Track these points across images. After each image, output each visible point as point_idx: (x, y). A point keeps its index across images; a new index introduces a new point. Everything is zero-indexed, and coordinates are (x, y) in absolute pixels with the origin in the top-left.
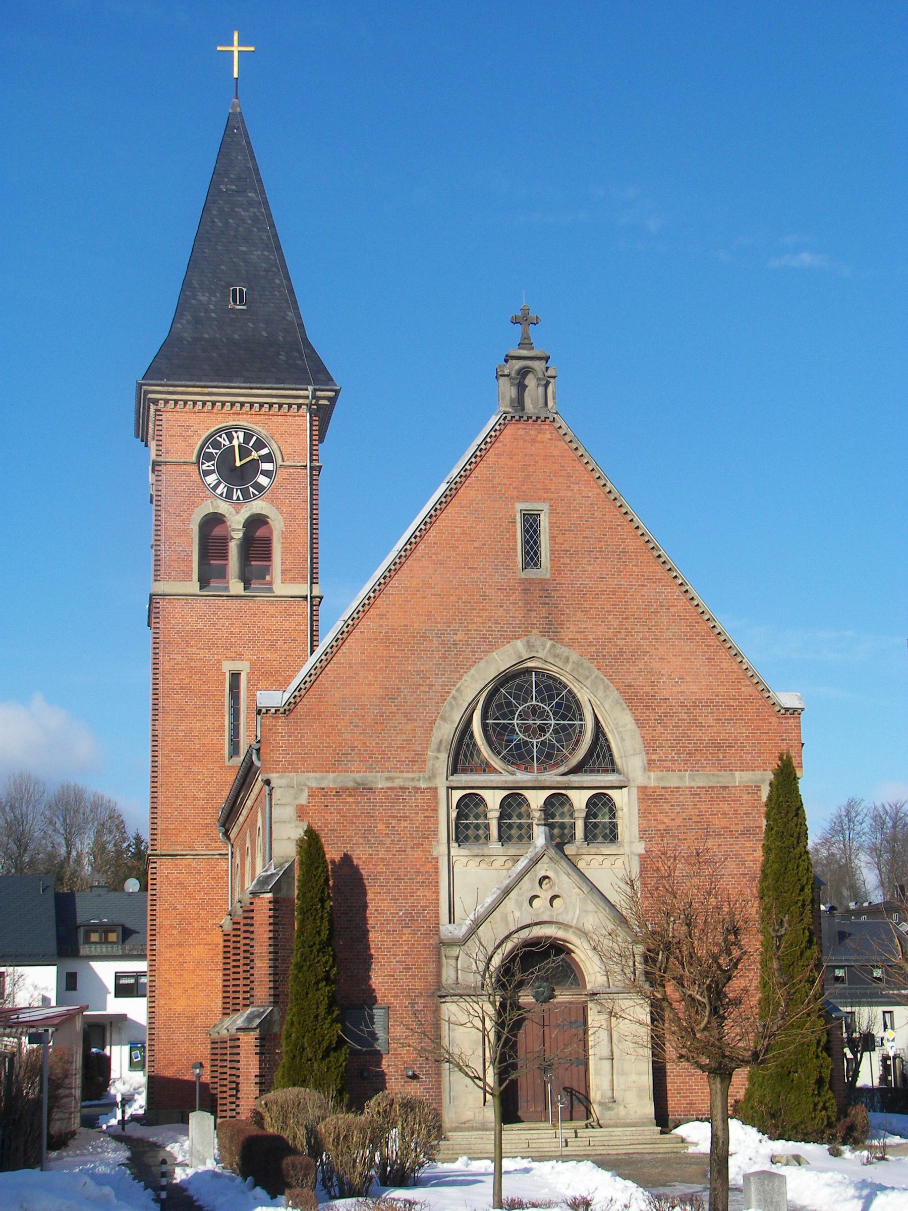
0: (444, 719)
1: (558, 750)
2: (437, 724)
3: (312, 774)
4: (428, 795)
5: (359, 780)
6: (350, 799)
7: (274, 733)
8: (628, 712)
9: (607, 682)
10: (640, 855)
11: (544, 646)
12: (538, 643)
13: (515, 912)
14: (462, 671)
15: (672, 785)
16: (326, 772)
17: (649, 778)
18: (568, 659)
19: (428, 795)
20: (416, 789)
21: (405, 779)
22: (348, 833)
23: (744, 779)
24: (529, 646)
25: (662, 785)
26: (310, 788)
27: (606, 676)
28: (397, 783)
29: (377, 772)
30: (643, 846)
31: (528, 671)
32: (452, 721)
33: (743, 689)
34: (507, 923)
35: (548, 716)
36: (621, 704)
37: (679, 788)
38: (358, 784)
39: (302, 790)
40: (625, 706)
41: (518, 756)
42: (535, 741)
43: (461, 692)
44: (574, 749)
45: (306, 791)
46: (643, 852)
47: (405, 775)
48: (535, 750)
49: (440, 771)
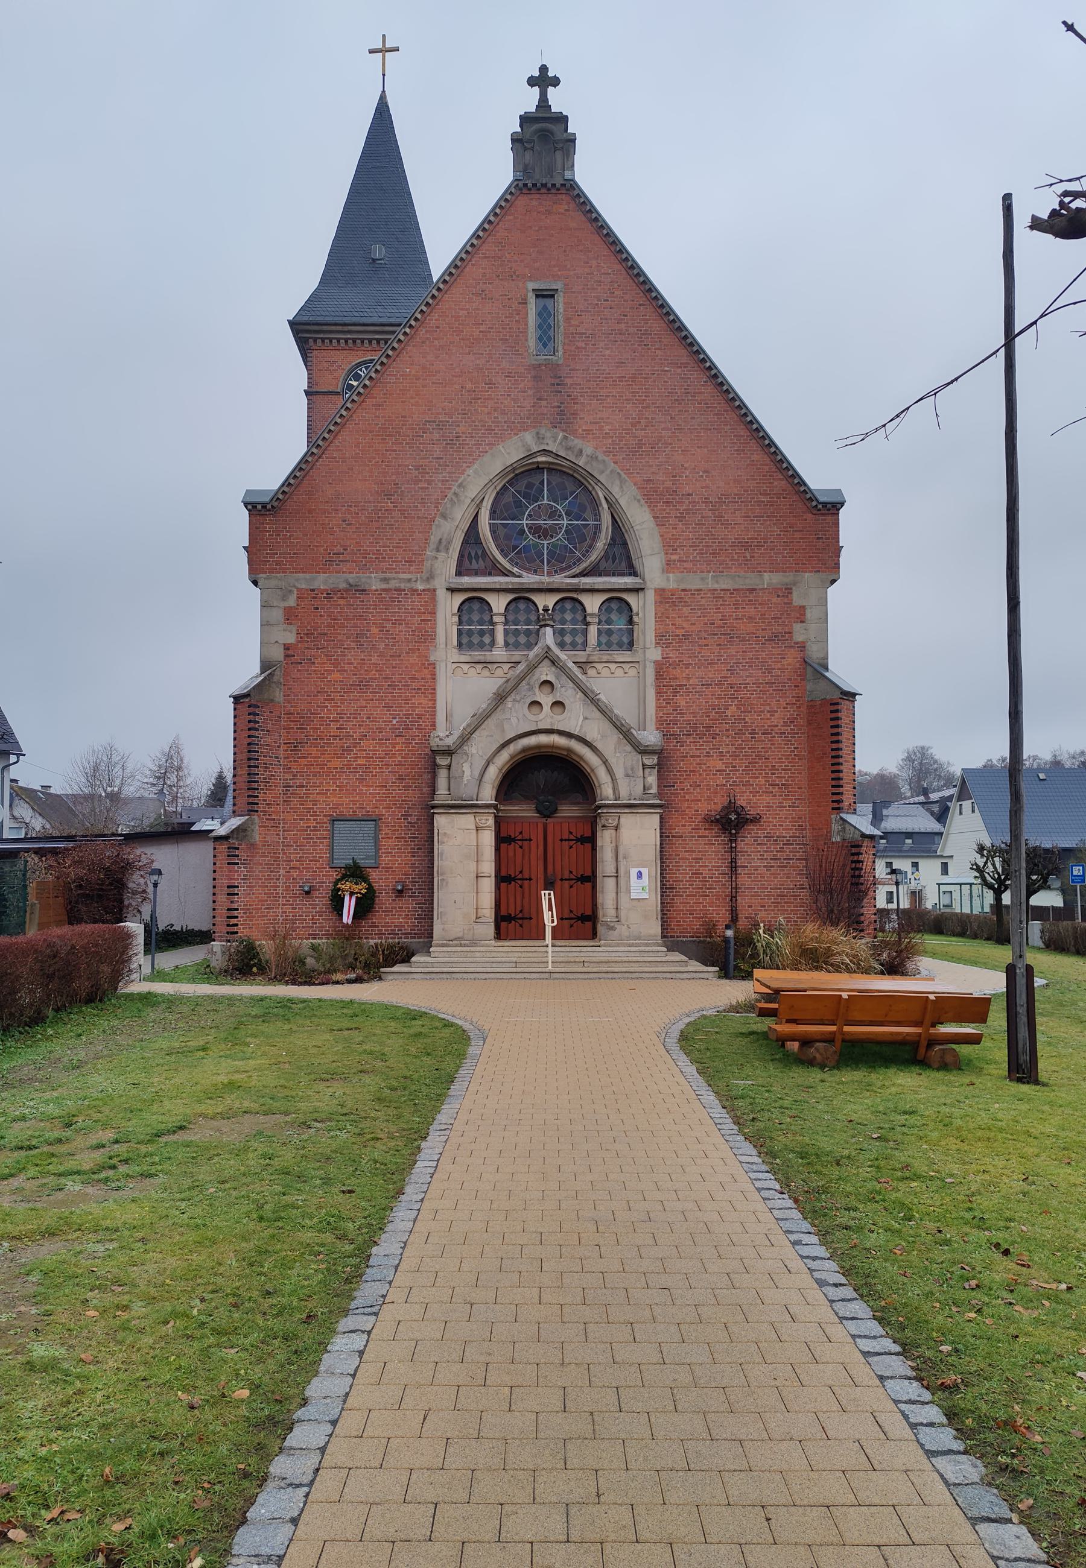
0: (444, 517)
1: (571, 552)
2: (436, 522)
3: (301, 575)
4: (426, 597)
5: (351, 581)
6: (342, 602)
8: (646, 508)
9: (623, 476)
10: (656, 662)
11: (555, 438)
12: (548, 435)
13: (517, 719)
17: (668, 579)
18: (581, 451)
19: (426, 597)
20: (414, 591)
21: (401, 580)
23: (774, 581)
24: (539, 438)
26: (298, 589)
28: (393, 584)
30: (660, 652)
31: (538, 468)
34: (503, 731)
35: (560, 516)
36: (639, 501)
38: (351, 586)
40: (643, 502)
41: (529, 559)
42: (545, 542)
44: (587, 551)
46: (659, 658)
47: (402, 576)
49: (438, 572)
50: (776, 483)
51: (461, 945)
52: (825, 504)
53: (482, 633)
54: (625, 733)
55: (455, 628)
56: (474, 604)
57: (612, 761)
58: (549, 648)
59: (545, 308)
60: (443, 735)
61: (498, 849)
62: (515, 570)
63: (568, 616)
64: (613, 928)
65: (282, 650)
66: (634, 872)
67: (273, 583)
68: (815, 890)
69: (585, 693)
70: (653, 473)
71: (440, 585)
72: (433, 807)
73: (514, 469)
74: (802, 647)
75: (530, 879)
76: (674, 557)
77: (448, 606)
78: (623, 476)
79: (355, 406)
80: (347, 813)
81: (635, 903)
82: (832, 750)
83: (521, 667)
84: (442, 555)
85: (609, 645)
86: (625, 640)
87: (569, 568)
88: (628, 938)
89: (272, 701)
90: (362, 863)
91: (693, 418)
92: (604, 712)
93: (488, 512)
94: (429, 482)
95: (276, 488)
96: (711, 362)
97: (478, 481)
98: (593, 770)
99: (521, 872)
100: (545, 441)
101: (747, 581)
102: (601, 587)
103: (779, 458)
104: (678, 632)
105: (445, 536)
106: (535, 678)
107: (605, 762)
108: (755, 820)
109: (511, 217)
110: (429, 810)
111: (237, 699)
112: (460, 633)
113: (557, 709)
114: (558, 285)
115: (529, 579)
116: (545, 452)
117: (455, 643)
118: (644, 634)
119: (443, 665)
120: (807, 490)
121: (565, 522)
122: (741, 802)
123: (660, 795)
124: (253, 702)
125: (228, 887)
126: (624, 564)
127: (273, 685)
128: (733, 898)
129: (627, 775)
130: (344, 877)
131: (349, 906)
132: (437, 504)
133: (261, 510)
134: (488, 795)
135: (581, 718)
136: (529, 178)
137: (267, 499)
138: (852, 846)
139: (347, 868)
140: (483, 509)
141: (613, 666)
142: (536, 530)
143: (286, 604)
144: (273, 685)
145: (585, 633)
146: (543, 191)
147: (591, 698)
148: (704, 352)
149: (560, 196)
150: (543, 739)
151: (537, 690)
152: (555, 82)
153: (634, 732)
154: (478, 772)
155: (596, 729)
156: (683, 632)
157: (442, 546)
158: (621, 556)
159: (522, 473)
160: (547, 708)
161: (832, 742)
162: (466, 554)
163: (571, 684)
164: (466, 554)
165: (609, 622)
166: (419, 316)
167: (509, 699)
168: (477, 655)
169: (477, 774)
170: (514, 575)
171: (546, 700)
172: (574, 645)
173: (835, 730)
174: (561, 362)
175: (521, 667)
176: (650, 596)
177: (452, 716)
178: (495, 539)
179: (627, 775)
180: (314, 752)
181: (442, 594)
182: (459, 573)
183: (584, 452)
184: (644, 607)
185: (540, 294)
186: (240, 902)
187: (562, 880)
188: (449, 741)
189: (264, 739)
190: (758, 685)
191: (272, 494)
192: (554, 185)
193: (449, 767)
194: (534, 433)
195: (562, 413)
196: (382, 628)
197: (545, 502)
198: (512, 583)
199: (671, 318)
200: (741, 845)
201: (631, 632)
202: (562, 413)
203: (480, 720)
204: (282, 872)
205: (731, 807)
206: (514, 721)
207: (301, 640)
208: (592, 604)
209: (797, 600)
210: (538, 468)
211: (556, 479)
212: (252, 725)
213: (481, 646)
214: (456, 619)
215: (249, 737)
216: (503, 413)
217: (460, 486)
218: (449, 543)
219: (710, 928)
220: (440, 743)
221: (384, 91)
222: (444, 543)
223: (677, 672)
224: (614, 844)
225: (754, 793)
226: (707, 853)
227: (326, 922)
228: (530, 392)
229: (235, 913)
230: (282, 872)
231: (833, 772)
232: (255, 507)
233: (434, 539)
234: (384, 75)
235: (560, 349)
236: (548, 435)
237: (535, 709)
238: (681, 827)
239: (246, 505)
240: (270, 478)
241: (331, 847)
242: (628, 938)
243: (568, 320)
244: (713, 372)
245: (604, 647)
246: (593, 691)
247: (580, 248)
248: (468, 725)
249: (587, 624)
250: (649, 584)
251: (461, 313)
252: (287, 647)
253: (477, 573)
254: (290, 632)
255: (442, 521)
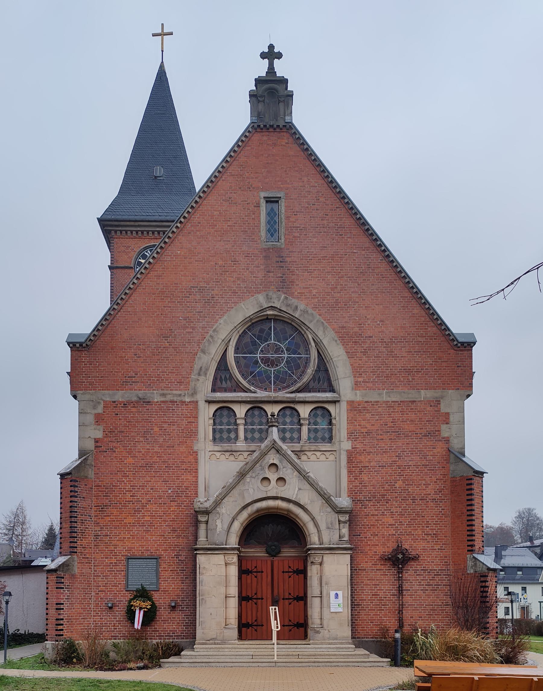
0: (203, 352)
1: (290, 376)
2: (198, 356)
5: (140, 396)
6: (134, 410)
7: (80, 362)
8: (341, 346)
9: (326, 324)
10: (348, 451)
13: (253, 489)
14: (217, 317)
15: (373, 400)
16: (117, 390)
17: (356, 395)
18: (296, 307)
20: (183, 402)
22: (132, 434)
23: (428, 396)
25: (366, 399)
26: (104, 401)
27: (325, 320)
28: (169, 398)
29: (154, 390)
30: (350, 445)
31: (268, 319)
32: (209, 354)
33: (429, 329)
34: (244, 498)
35: (282, 351)
36: (336, 341)
37: (378, 402)
38: (140, 399)
39: (99, 403)
40: (339, 342)
41: (261, 381)
42: (272, 369)
43: (217, 332)
44: (301, 375)
45: (102, 403)
46: (350, 448)
47: (174, 392)
48: (272, 376)
50: (429, 329)
51: (215, 644)
52: (462, 344)
53: (229, 431)
54: (327, 499)
55: (211, 428)
56: (224, 411)
57: (318, 518)
58: (275, 441)
59: (272, 209)
60: (203, 500)
61: (240, 578)
62: (252, 388)
63: (288, 420)
64: (318, 632)
65: (93, 442)
66: (332, 594)
67: (87, 397)
68: (456, 606)
69: (299, 472)
70: (346, 322)
71: (201, 398)
72: (196, 550)
73: (251, 320)
74: (447, 440)
75: (262, 599)
76: (360, 379)
77: (206, 413)
78: (326, 324)
79: (143, 276)
80: (138, 554)
81: (334, 615)
82: (468, 510)
83: (256, 455)
84: (202, 378)
85: (316, 439)
86: (327, 436)
87: (288, 386)
88: (329, 639)
89: (86, 477)
90: (147, 587)
91: (373, 285)
92: (313, 485)
93: (233, 349)
94: (193, 328)
95: (89, 332)
96: (385, 246)
97: (226, 328)
98: (305, 525)
99: (256, 594)
100: (272, 300)
101: (410, 396)
102: (310, 400)
103: (431, 312)
104: (362, 430)
105: (204, 365)
106: (265, 461)
107: (313, 519)
108: (415, 558)
109: (249, 148)
110: (193, 552)
111: (63, 476)
112: (214, 431)
113: (281, 483)
114: (281, 194)
115: (261, 394)
116: (273, 308)
117: (211, 438)
118: (340, 432)
119: (203, 453)
120: (451, 334)
121: (286, 356)
122: (406, 546)
123: (350, 541)
124: (73, 478)
125: (57, 604)
126: (326, 384)
127: (87, 467)
128: (400, 612)
129: (328, 528)
130: (135, 597)
131: (139, 617)
132: (199, 343)
133: (79, 347)
134: (233, 541)
135: (297, 489)
136: (261, 121)
137: (83, 340)
138: (481, 576)
139: (137, 591)
140: (230, 347)
141: (318, 454)
142: (266, 361)
143: (96, 412)
144: (87, 467)
145: (299, 431)
146: (271, 130)
147: (304, 476)
148: (381, 240)
149: (282, 134)
150: (271, 503)
151: (267, 470)
152: (279, 56)
153: (333, 499)
154: (227, 525)
155: (307, 497)
156: (366, 430)
157: (202, 372)
158: (324, 379)
159: (256, 322)
160: (273, 482)
161: (468, 505)
162: (219, 377)
163: (290, 466)
164: (219, 377)
165: (316, 423)
166: (186, 215)
167: (248, 476)
168: (226, 446)
169: (226, 527)
170: (251, 391)
171: (273, 476)
172: (292, 439)
173: (469, 497)
174: (283, 246)
175: (256, 455)
176: (344, 406)
177: (209, 487)
178: (238, 367)
179: (328, 528)
180: (115, 512)
181: (202, 405)
182: (214, 390)
183: (300, 308)
184: (340, 414)
185: (269, 201)
186: (64, 614)
187: (283, 599)
188: (207, 505)
189: (81, 503)
190: (417, 466)
191: (86, 337)
192: (278, 126)
193: (207, 522)
194: (265, 295)
195: (283, 281)
196: (161, 428)
197: (272, 342)
198: (250, 397)
199: (358, 216)
200: (406, 575)
201: (331, 430)
202: (283, 281)
203: (228, 491)
204: (93, 594)
205: (399, 549)
206: (251, 491)
207: (106, 436)
208: (304, 411)
209: (444, 409)
210: (267, 319)
211: (280, 326)
212: (73, 494)
213: (229, 440)
214: (211, 421)
215: (71, 502)
216: (244, 281)
217: (214, 331)
218: (207, 370)
219: (384, 632)
220: (201, 506)
221: (162, 62)
222: (203, 369)
223: (362, 458)
224: (319, 575)
225: (415, 540)
226: (383, 581)
227: (123, 628)
228: (262, 267)
229: (62, 622)
230: (93, 594)
231: (468, 526)
232: (74, 345)
233: (196, 367)
234: (162, 51)
235: (283, 237)
236: (274, 296)
237: (266, 483)
238: (365, 563)
239: (69, 344)
240: (86, 327)
241: (127, 577)
242: (329, 639)
243: (288, 218)
244: (386, 253)
245: (312, 440)
246: (305, 471)
247: (296, 169)
248: (220, 494)
249: (301, 425)
250: (343, 398)
251: (215, 213)
252: (96, 441)
253: (225, 390)
254: (99, 430)
255: (202, 355)
